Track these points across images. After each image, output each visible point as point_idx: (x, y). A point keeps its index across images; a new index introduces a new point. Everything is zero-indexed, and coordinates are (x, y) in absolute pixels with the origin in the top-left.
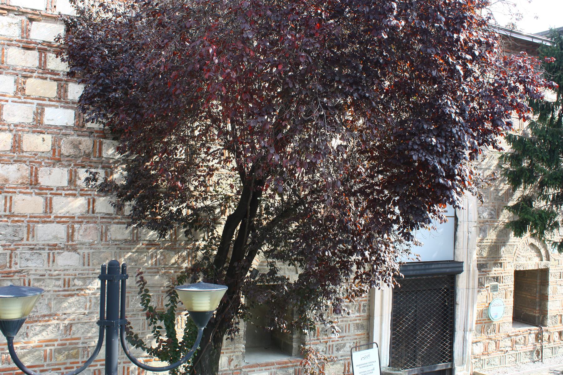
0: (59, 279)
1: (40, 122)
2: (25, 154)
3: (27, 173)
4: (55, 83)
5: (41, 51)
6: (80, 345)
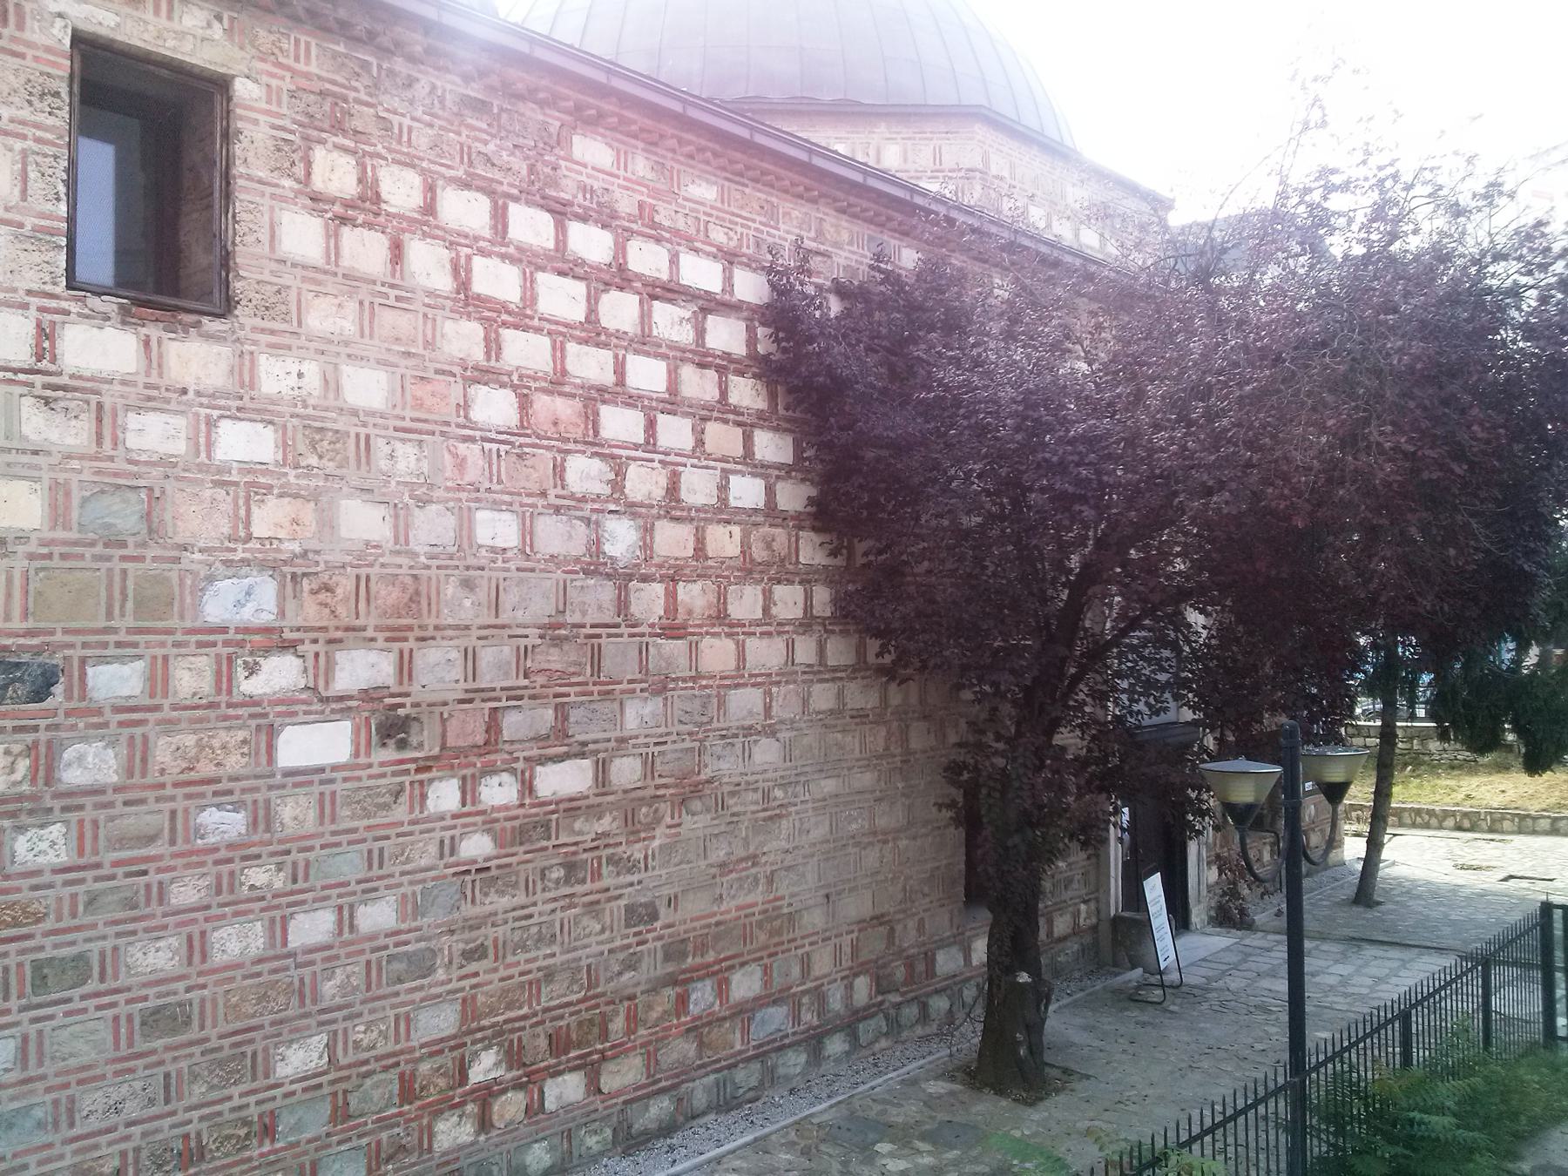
0: (755, 790)
1: (723, 500)
2: (710, 563)
3: (713, 598)
4: (739, 431)
5: (722, 371)
6: (785, 911)
